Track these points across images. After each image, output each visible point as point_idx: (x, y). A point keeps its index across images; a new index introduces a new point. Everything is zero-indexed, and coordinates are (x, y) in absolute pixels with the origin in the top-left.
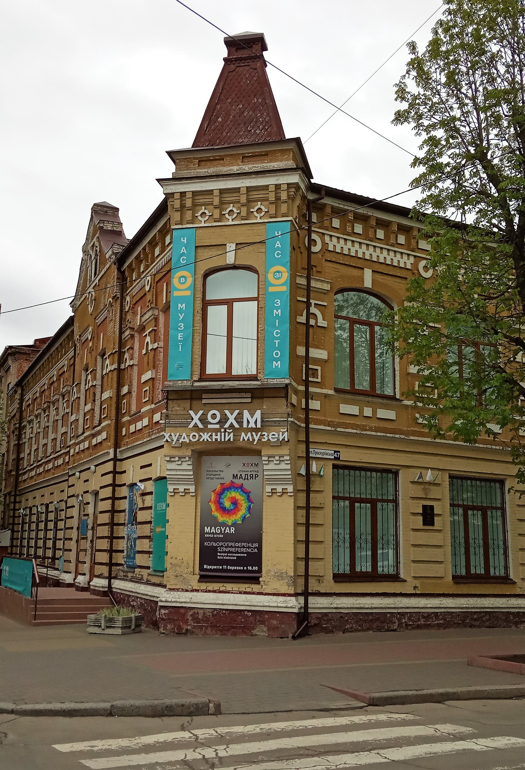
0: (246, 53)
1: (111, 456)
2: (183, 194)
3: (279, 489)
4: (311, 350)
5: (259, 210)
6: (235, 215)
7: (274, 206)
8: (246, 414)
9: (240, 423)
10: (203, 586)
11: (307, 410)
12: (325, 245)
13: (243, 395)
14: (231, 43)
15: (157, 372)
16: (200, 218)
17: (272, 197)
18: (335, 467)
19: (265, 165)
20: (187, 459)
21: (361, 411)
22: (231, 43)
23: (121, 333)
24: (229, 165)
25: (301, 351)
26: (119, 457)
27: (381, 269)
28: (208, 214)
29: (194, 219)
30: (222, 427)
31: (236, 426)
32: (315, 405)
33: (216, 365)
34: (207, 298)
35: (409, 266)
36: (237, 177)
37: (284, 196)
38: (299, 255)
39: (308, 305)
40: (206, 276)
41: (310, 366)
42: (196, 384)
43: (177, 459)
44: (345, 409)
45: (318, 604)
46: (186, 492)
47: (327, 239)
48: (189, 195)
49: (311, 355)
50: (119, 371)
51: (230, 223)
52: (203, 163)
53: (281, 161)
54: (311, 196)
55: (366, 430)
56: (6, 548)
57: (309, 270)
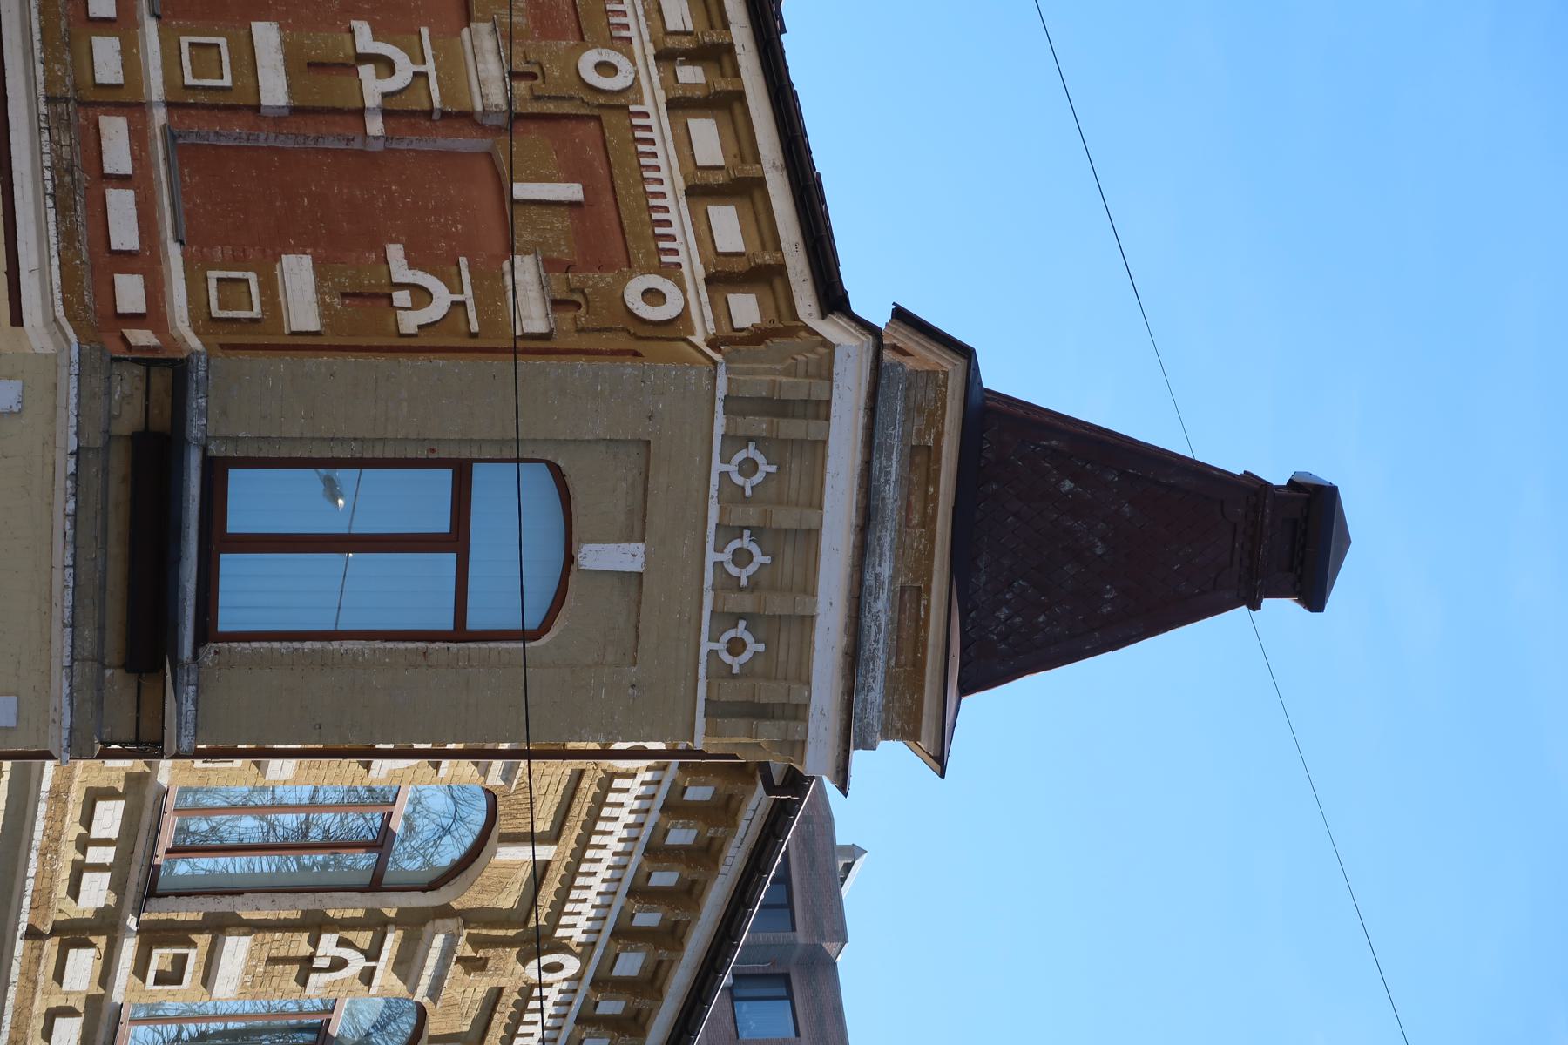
0: (1280, 541)
2: (821, 409)
6: (733, 570)
15: (279, 119)
16: (741, 456)
33: (255, 500)
35: (560, 933)
37: (769, 731)
40: (555, 470)
42: (194, 460)
48: (812, 429)
51: (711, 557)
53: (886, 709)
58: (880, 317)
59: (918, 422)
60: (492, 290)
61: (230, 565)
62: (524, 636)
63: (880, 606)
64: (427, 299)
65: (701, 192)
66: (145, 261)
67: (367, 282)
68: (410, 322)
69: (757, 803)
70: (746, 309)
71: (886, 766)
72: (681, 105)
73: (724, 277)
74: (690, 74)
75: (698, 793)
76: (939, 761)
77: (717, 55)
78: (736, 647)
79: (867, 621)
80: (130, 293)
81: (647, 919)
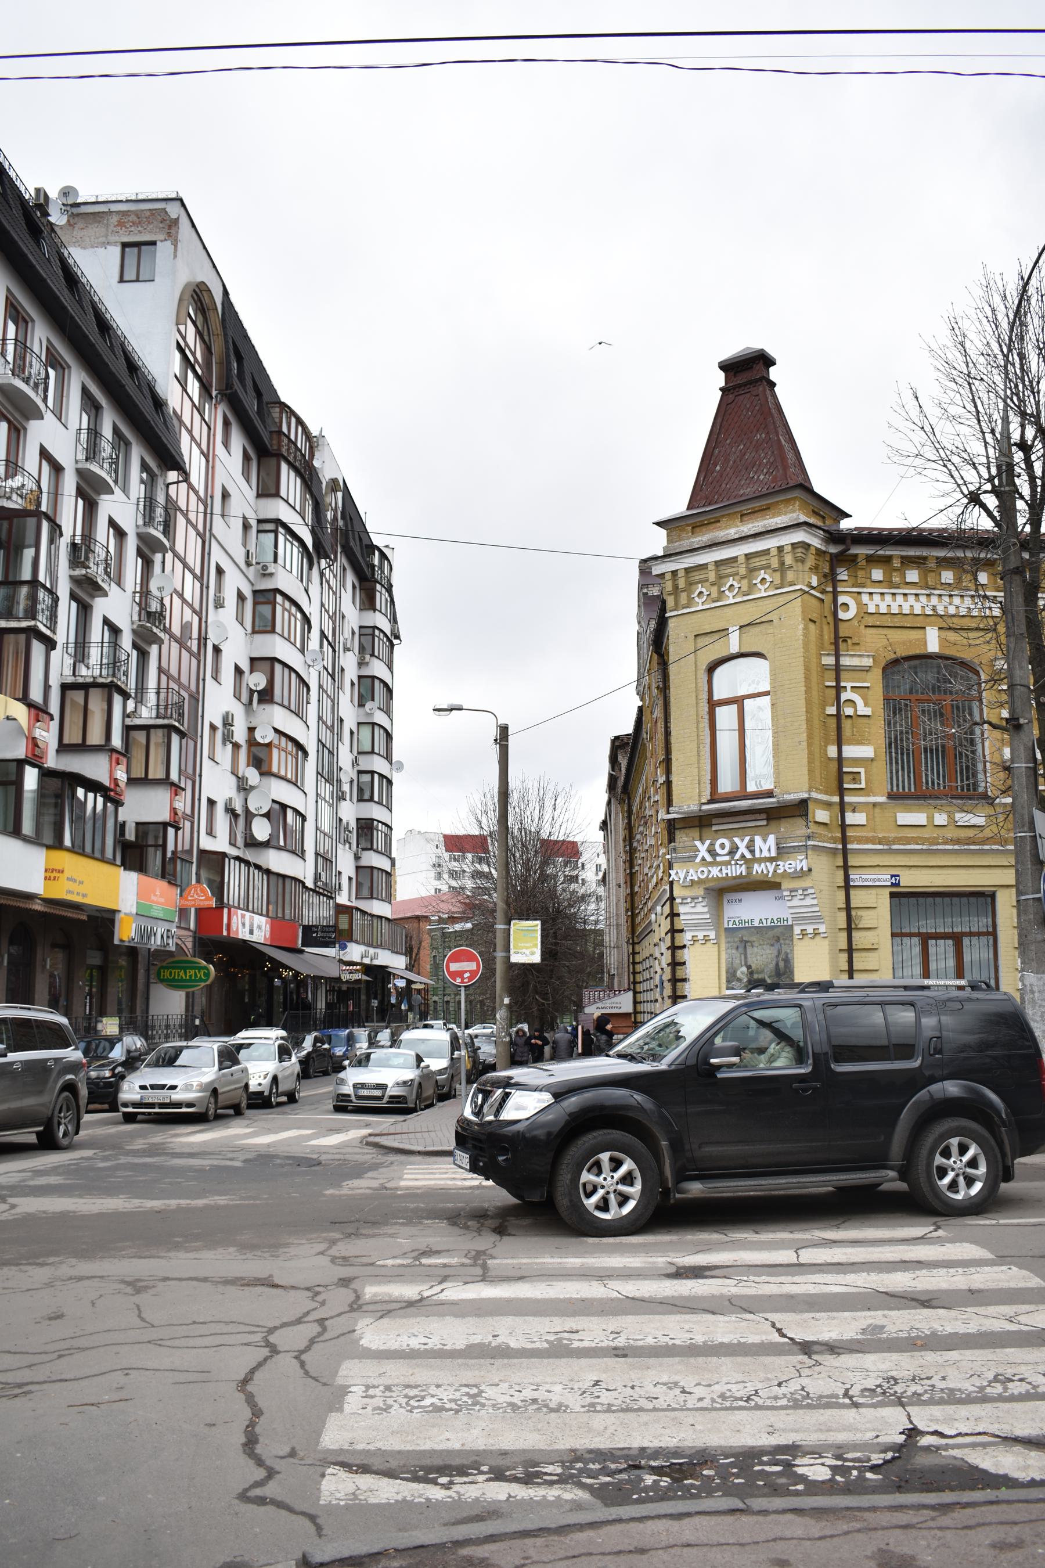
1: (668, 895)
2: (674, 573)
3: (810, 930)
4: (845, 748)
7: (778, 574)
8: (758, 839)
9: (752, 852)
11: (843, 826)
12: (861, 605)
13: (757, 816)
14: (729, 367)
17: (775, 563)
18: (892, 895)
19: (766, 522)
20: (700, 899)
21: (931, 819)
22: (729, 367)
24: (726, 528)
25: (832, 751)
27: (957, 623)
28: (706, 593)
29: (690, 602)
30: (732, 858)
31: (748, 856)
32: (851, 818)
34: (716, 698)
36: (740, 538)
37: (789, 560)
38: (825, 628)
39: (839, 689)
41: (845, 770)
42: (704, 807)
43: (689, 900)
44: (905, 818)
46: (706, 939)
47: (865, 598)
48: (681, 574)
49: (845, 755)
51: (731, 601)
52: (697, 530)
54: (833, 549)
55: (939, 844)
57: (838, 642)
59: (684, 535)
61: (751, 787)
63: (747, 528)
79: (751, 533)
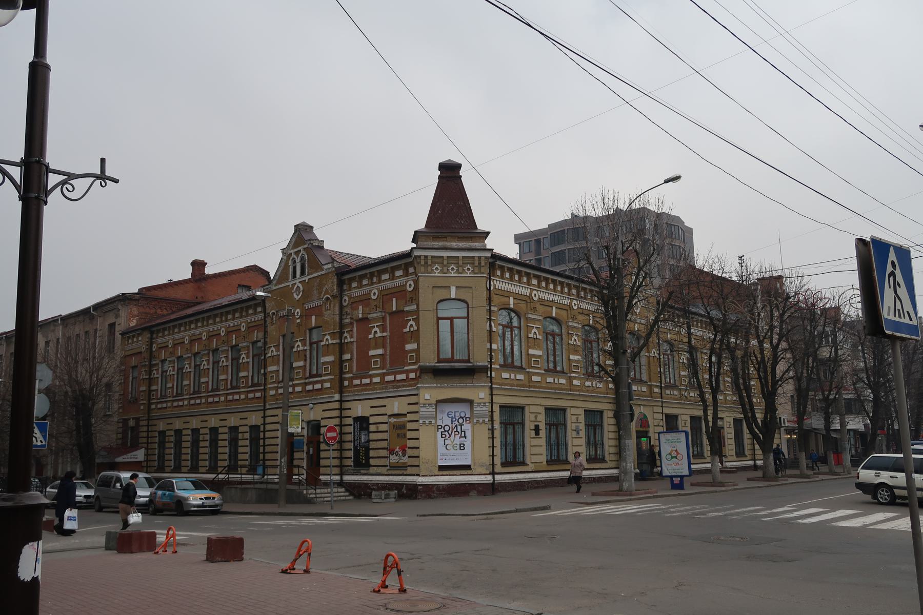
0: (450, 173)
5: (468, 269)
10: (441, 473)
11: (491, 377)
14: (443, 167)
15: (386, 351)
22: (443, 167)
23: (341, 319)
26: (344, 399)
33: (446, 353)
37: (483, 263)
40: (439, 302)
45: (498, 478)
50: (341, 345)
56: (141, 462)
58: (414, 245)
60: (410, 313)
62: (468, 308)
64: (411, 326)
65: (393, 278)
66: (407, 372)
67: (409, 335)
68: (415, 328)
69: (498, 263)
70: (411, 270)
71: (489, 243)
72: (380, 281)
73: (406, 274)
74: (375, 280)
75: (499, 273)
76: (488, 233)
77: (372, 274)
78: (468, 269)
80: (412, 375)
81: (525, 280)
